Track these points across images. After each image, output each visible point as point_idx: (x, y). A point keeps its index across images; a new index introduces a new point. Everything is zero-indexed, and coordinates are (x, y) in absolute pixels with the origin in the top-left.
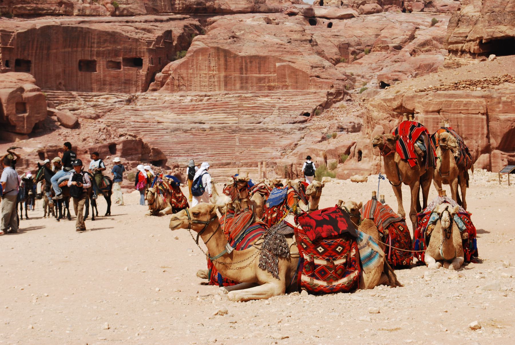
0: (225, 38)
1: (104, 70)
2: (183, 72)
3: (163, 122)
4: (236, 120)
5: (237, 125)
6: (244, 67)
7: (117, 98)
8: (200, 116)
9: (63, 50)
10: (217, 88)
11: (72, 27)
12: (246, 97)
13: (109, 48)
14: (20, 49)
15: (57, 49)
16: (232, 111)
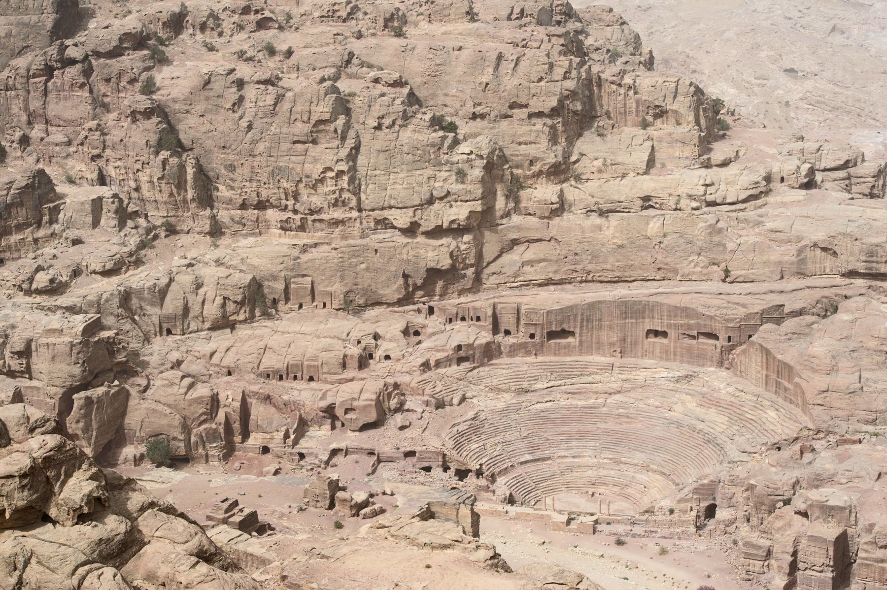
1: (675, 342)
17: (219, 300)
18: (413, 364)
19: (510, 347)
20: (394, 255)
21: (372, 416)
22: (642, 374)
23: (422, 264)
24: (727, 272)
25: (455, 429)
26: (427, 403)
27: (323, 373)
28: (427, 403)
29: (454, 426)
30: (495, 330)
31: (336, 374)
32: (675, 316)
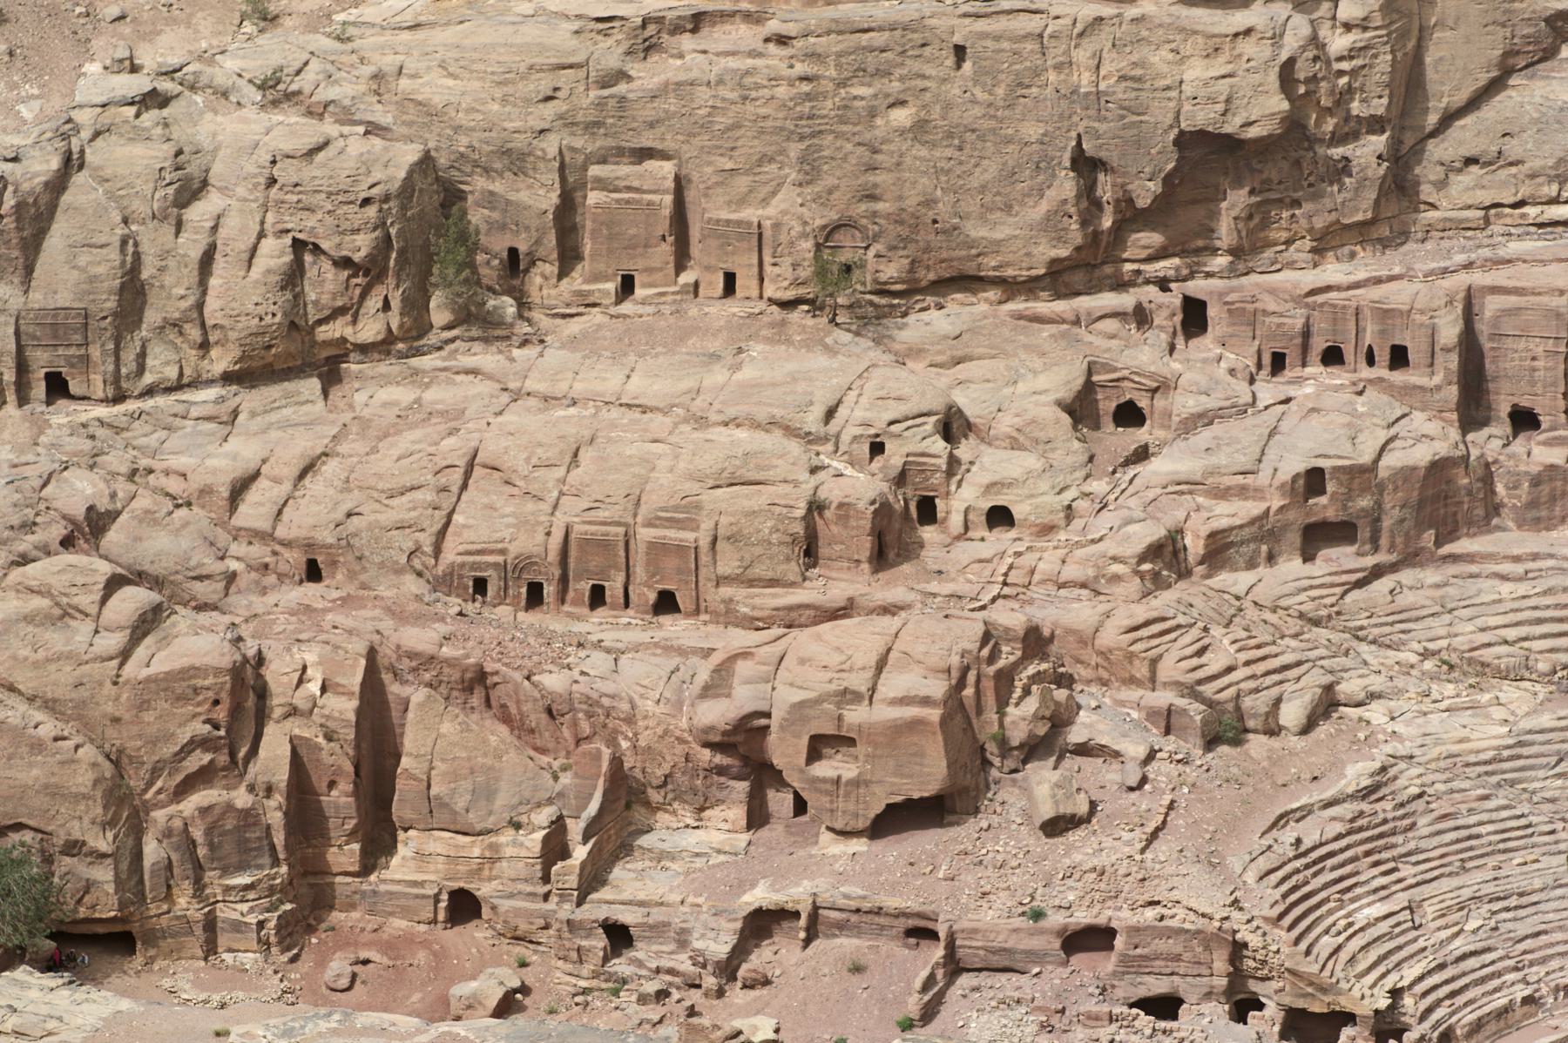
17: (274, 254)
18: (1110, 547)
19: (1536, 482)
20: (1037, 72)
21: (929, 773)
23: (1160, 113)
25: (1288, 835)
26: (1168, 721)
27: (720, 581)
28: (1168, 721)
29: (1281, 820)
30: (1472, 406)
31: (773, 583)
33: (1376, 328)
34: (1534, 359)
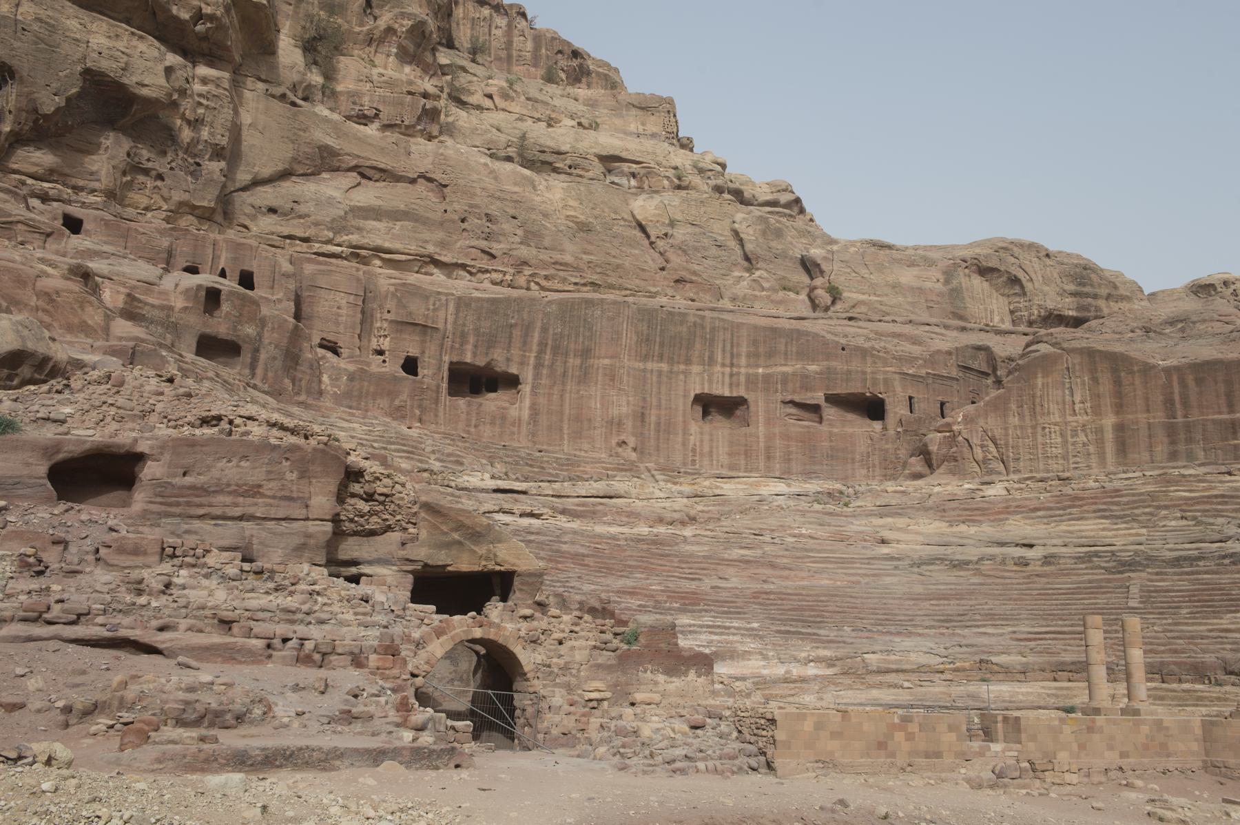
0: (1119, 330)
2: (992, 423)
3: (898, 542)
4: (1138, 535)
5: (1141, 547)
6: (1177, 398)
7: (789, 485)
8: (1018, 528)
9: (641, 365)
10: (1094, 461)
11: (670, 313)
12: (1184, 476)
13: (785, 369)
14: (472, 340)
15: (612, 358)
16: (1128, 512)
19: (352, 377)
22: (726, 486)
24: (835, 294)
32: (771, 354)
33: (230, 255)
34: (339, 308)
